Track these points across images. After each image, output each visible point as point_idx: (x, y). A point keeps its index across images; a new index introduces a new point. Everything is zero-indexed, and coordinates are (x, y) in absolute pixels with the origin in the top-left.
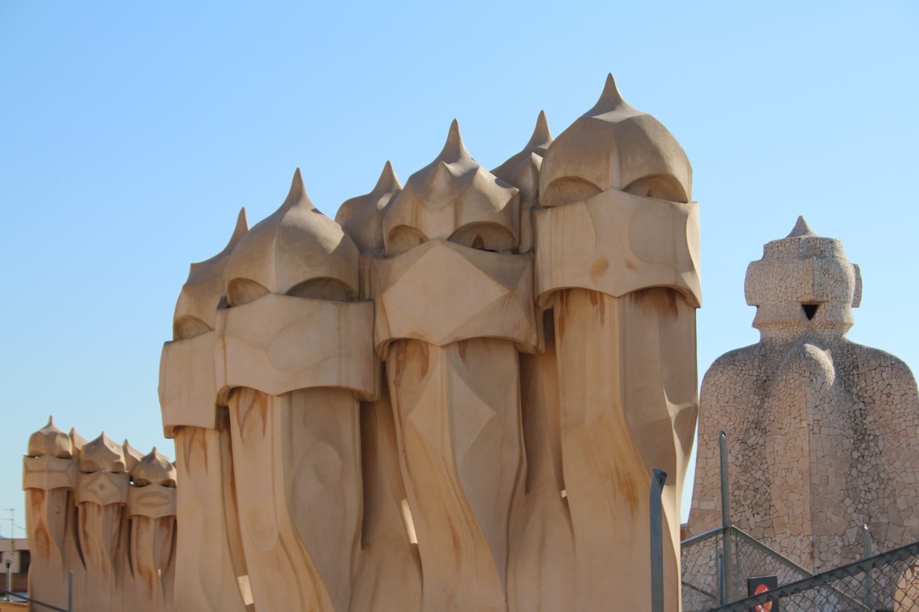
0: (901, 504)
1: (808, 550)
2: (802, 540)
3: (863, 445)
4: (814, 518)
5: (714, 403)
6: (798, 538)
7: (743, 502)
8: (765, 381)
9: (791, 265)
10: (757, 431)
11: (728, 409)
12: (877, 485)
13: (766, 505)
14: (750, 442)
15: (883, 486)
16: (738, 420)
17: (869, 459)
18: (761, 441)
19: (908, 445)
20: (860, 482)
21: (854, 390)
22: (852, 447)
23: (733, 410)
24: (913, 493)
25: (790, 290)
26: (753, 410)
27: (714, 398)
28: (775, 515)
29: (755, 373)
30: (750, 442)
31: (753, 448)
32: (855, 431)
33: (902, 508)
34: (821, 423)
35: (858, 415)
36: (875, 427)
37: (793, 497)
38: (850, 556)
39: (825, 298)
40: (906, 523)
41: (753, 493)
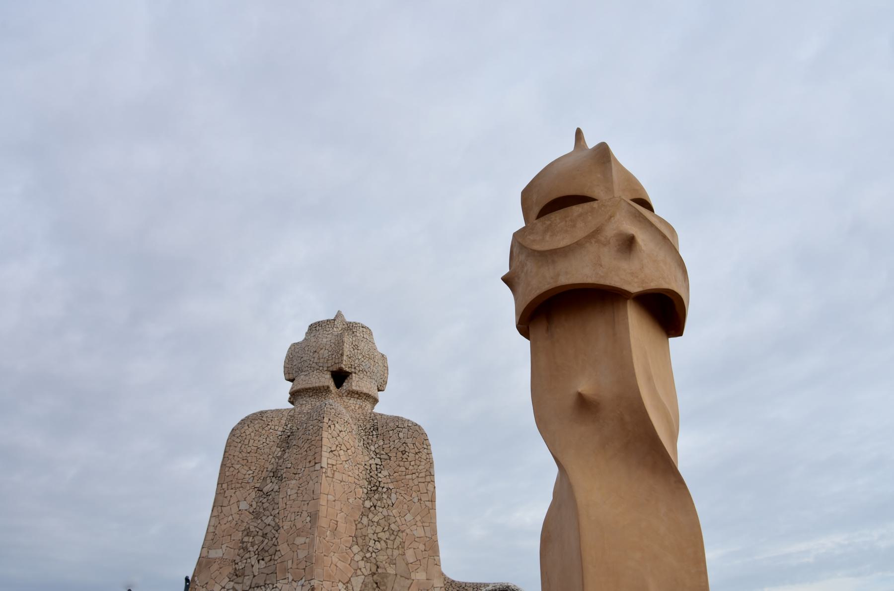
0: (410, 556)
2: (303, 586)
5: (237, 454)
7: (251, 549)
9: (325, 340)
10: (274, 479)
11: (249, 458)
12: (387, 535)
13: (272, 551)
14: (265, 490)
15: (392, 537)
16: (258, 469)
17: (381, 510)
23: (254, 460)
24: (422, 547)
25: (322, 360)
26: (273, 460)
27: (238, 449)
28: (279, 561)
29: (281, 429)
30: (265, 490)
31: (267, 494)
32: (370, 483)
34: (335, 468)
40: (413, 576)
41: (262, 539)
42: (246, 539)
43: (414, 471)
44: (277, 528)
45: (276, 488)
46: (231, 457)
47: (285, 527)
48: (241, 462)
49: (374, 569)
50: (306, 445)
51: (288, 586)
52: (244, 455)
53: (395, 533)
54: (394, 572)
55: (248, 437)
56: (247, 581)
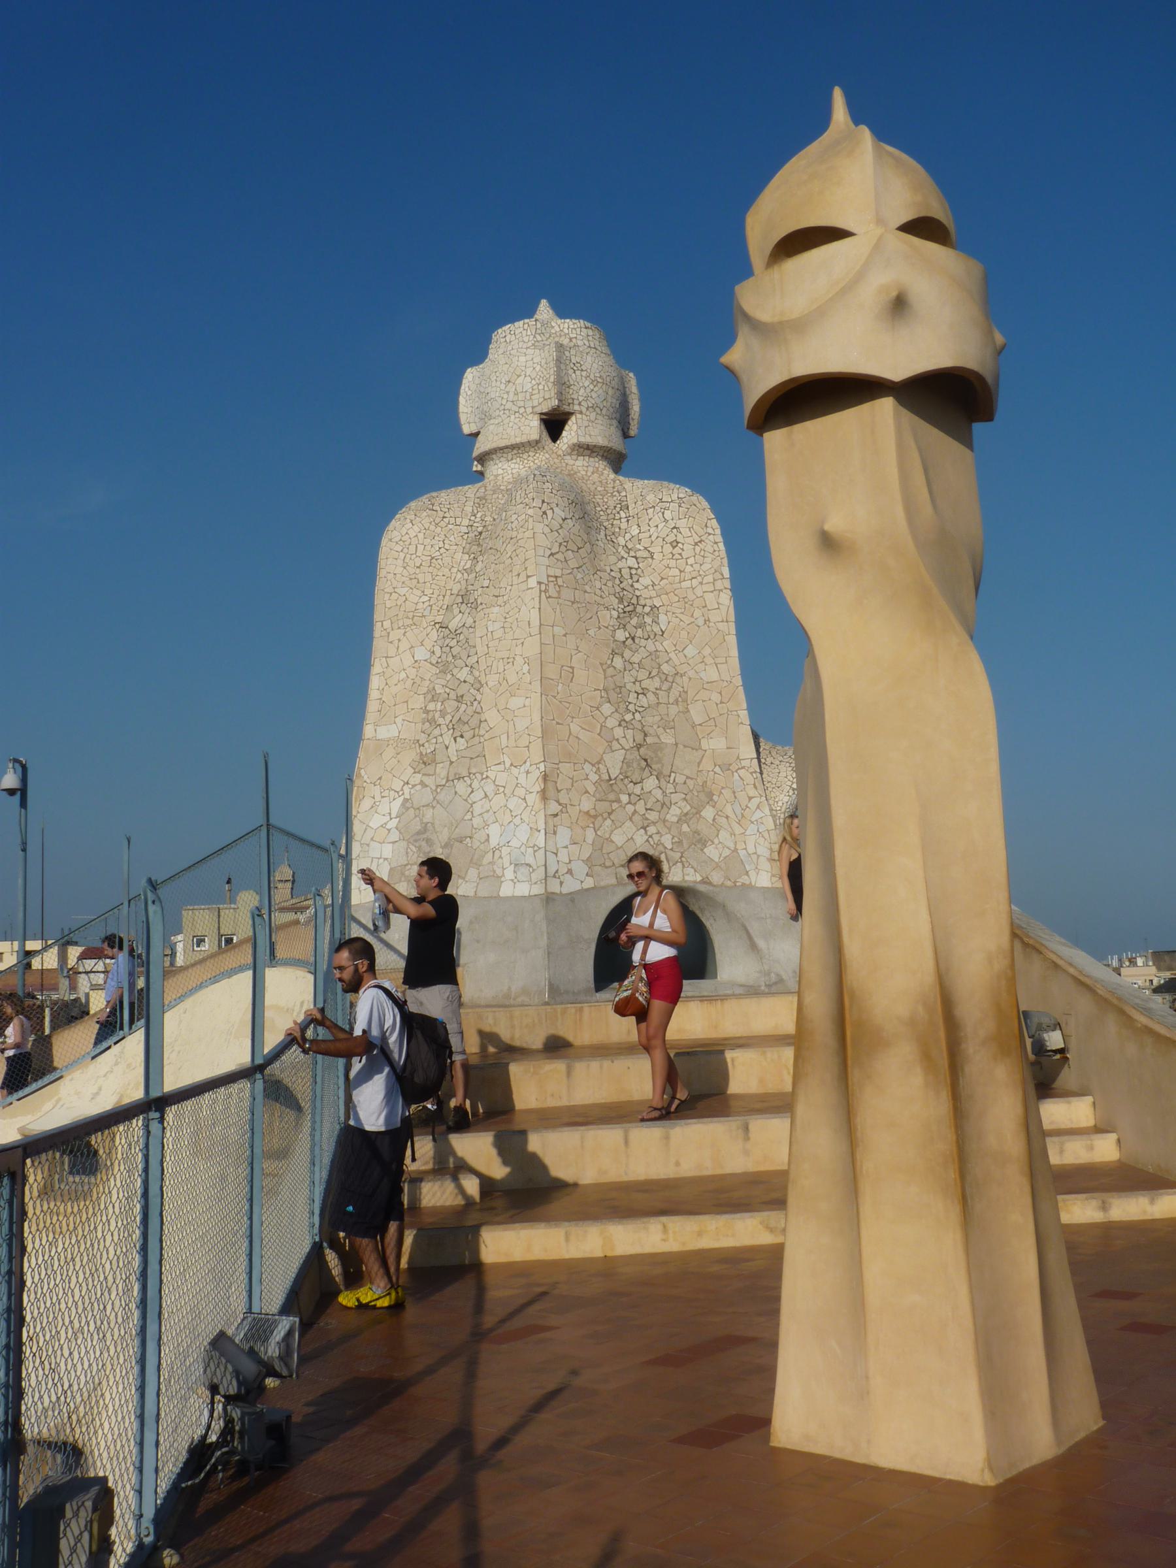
1: (537, 788)
2: (528, 772)
3: (634, 621)
4: (546, 734)
5: (399, 570)
6: (522, 769)
7: (441, 721)
8: (480, 533)
9: (523, 359)
11: (421, 577)
12: (656, 683)
13: (474, 722)
14: (453, 625)
18: (470, 621)
19: (707, 621)
20: (628, 678)
21: (621, 541)
22: (613, 622)
23: (429, 578)
24: (716, 697)
25: (521, 397)
26: (459, 575)
27: (400, 562)
28: (486, 737)
29: (466, 522)
30: (453, 625)
31: (457, 633)
32: (621, 600)
33: (698, 720)
34: (560, 581)
35: (627, 576)
36: (653, 594)
37: (516, 702)
38: (612, 796)
39: (577, 408)
40: (704, 744)
41: (456, 704)
42: (431, 706)
43: (694, 574)
44: (479, 686)
45: (470, 621)
46: (390, 576)
47: (491, 684)
48: (408, 583)
49: (639, 738)
50: (510, 548)
51: (505, 775)
52: (412, 571)
53: (670, 679)
54: (671, 741)
55: (414, 541)
56: (441, 771)
